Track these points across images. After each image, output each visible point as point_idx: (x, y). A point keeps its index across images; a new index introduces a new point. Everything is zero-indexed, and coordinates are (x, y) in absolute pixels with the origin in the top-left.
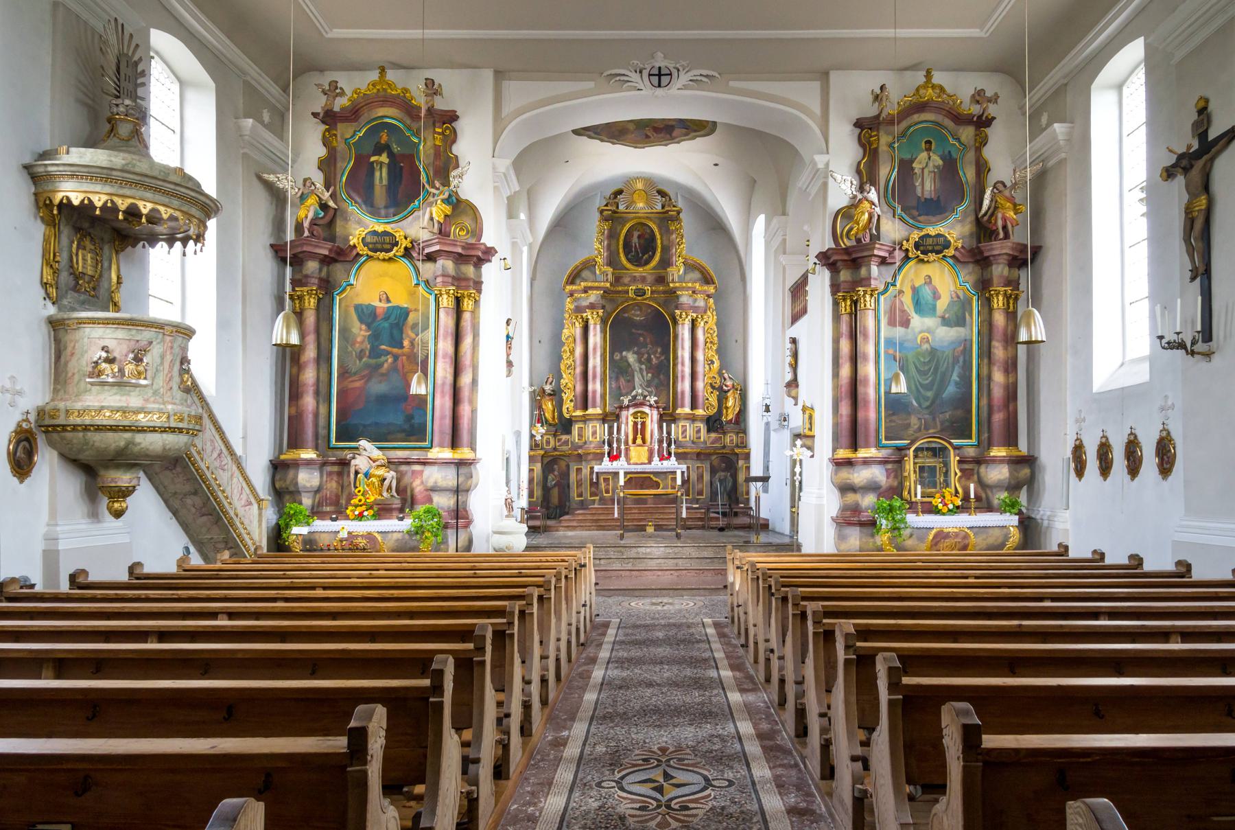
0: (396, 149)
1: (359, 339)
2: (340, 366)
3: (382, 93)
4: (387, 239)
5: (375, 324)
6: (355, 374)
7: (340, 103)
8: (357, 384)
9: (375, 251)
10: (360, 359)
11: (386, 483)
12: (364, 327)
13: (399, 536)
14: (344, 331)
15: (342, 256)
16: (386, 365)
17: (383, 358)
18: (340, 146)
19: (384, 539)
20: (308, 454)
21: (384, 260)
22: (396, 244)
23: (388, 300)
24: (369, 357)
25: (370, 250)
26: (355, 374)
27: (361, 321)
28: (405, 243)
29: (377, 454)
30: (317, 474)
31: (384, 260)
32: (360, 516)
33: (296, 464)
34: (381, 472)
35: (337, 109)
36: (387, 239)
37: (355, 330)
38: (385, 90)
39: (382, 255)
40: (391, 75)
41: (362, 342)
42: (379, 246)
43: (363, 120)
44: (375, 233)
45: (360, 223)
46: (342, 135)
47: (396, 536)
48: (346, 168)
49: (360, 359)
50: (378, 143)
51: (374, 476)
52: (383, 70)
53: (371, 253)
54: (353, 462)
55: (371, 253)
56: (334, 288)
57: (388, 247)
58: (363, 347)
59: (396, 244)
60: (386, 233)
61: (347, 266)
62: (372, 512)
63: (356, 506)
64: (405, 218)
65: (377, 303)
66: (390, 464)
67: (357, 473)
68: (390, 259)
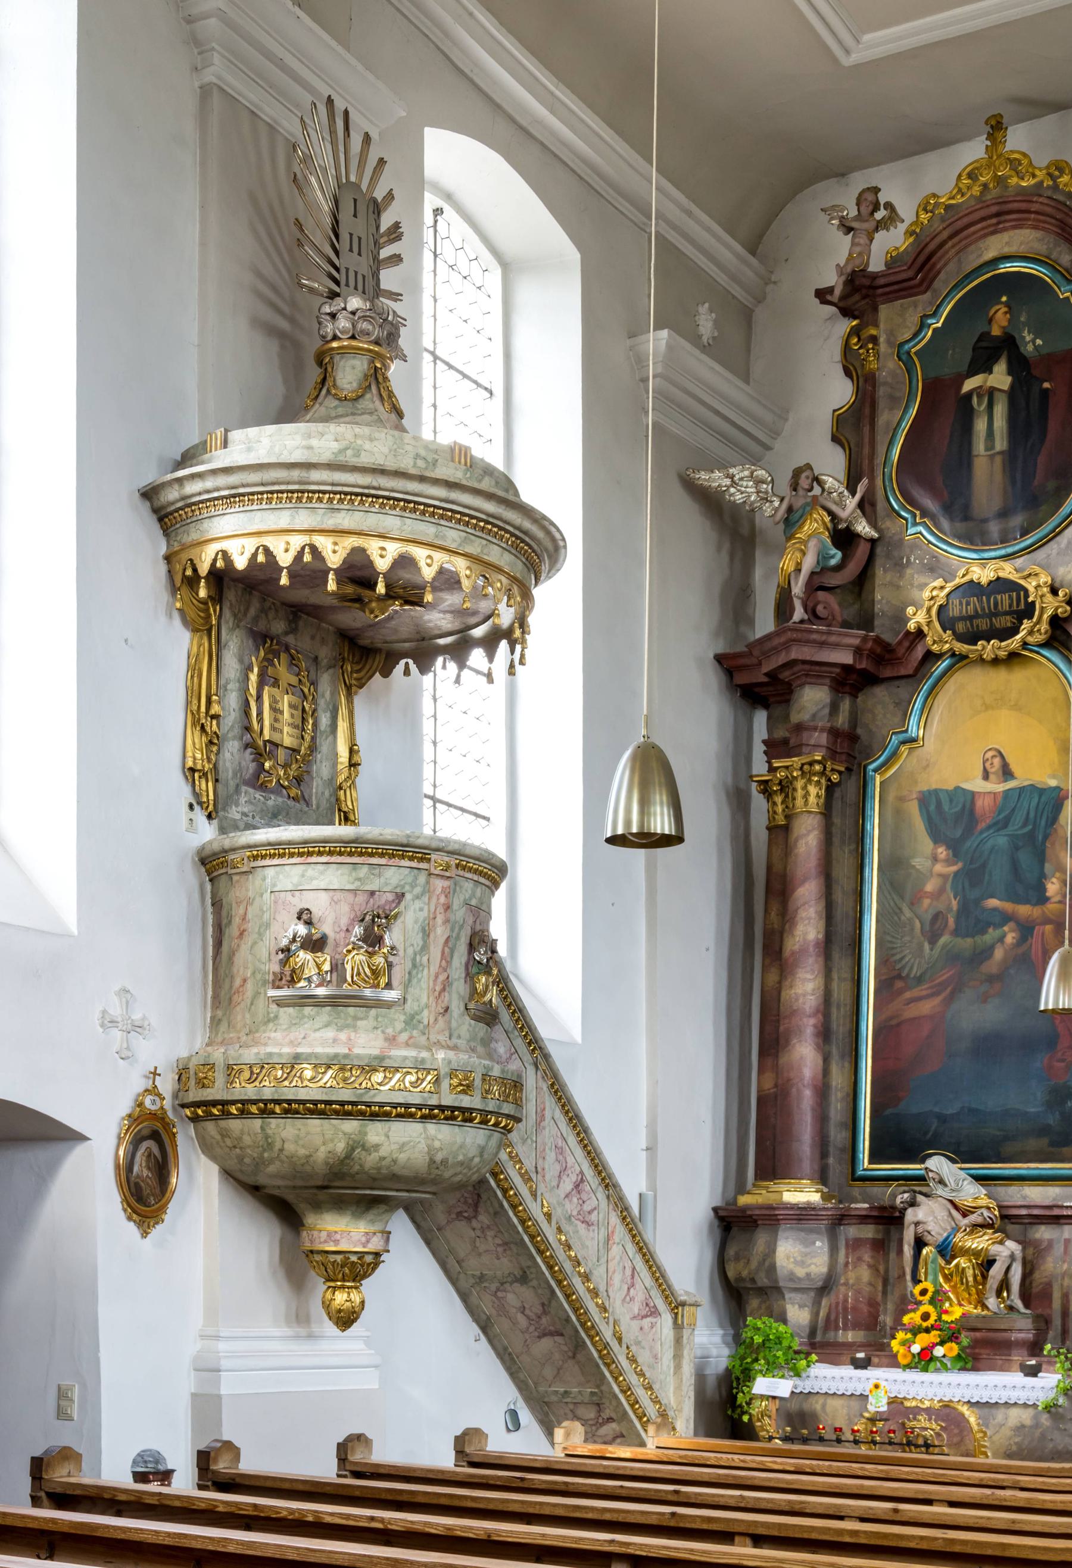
0: (1030, 343)
1: (929, 887)
2: (882, 961)
3: (994, 192)
4: (1004, 601)
5: (970, 844)
6: (919, 980)
7: (889, 244)
8: (927, 1007)
9: (972, 638)
10: (933, 940)
11: (996, 1272)
12: (942, 852)
13: (1026, 1417)
14: (892, 865)
15: (889, 665)
16: (999, 954)
17: (992, 934)
18: (886, 365)
19: (984, 1422)
20: (802, 1194)
21: (996, 661)
22: (1029, 611)
23: (1007, 773)
24: (956, 933)
25: (959, 638)
26: (919, 980)
27: (936, 836)
28: (1051, 606)
29: (971, 1193)
30: (821, 1245)
31: (996, 661)
32: (925, 1360)
33: (771, 1218)
34: (981, 1242)
35: (876, 265)
36: (1004, 601)
37: (920, 863)
38: (1000, 181)
39: (990, 648)
40: (1018, 138)
41: (941, 891)
42: (983, 624)
43: (943, 282)
44: (972, 588)
45: (934, 568)
46: (891, 334)
47: (1016, 1416)
48: (899, 421)
49: (933, 940)
50: (985, 336)
51: (965, 1252)
52: (996, 127)
53: (961, 647)
54: (910, 1215)
55: (961, 647)
56: (869, 754)
57: (1006, 621)
58: (941, 906)
59: (1029, 611)
60: (1001, 584)
61: (902, 690)
62: (953, 1349)
63: (916, 1331)
64: (1055, 533)
65: (977, 785)
66: (1007, 1221)
67: (920, 1243)
68: (1013, 656)
